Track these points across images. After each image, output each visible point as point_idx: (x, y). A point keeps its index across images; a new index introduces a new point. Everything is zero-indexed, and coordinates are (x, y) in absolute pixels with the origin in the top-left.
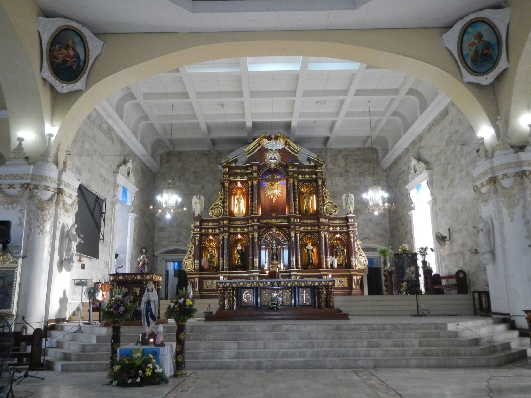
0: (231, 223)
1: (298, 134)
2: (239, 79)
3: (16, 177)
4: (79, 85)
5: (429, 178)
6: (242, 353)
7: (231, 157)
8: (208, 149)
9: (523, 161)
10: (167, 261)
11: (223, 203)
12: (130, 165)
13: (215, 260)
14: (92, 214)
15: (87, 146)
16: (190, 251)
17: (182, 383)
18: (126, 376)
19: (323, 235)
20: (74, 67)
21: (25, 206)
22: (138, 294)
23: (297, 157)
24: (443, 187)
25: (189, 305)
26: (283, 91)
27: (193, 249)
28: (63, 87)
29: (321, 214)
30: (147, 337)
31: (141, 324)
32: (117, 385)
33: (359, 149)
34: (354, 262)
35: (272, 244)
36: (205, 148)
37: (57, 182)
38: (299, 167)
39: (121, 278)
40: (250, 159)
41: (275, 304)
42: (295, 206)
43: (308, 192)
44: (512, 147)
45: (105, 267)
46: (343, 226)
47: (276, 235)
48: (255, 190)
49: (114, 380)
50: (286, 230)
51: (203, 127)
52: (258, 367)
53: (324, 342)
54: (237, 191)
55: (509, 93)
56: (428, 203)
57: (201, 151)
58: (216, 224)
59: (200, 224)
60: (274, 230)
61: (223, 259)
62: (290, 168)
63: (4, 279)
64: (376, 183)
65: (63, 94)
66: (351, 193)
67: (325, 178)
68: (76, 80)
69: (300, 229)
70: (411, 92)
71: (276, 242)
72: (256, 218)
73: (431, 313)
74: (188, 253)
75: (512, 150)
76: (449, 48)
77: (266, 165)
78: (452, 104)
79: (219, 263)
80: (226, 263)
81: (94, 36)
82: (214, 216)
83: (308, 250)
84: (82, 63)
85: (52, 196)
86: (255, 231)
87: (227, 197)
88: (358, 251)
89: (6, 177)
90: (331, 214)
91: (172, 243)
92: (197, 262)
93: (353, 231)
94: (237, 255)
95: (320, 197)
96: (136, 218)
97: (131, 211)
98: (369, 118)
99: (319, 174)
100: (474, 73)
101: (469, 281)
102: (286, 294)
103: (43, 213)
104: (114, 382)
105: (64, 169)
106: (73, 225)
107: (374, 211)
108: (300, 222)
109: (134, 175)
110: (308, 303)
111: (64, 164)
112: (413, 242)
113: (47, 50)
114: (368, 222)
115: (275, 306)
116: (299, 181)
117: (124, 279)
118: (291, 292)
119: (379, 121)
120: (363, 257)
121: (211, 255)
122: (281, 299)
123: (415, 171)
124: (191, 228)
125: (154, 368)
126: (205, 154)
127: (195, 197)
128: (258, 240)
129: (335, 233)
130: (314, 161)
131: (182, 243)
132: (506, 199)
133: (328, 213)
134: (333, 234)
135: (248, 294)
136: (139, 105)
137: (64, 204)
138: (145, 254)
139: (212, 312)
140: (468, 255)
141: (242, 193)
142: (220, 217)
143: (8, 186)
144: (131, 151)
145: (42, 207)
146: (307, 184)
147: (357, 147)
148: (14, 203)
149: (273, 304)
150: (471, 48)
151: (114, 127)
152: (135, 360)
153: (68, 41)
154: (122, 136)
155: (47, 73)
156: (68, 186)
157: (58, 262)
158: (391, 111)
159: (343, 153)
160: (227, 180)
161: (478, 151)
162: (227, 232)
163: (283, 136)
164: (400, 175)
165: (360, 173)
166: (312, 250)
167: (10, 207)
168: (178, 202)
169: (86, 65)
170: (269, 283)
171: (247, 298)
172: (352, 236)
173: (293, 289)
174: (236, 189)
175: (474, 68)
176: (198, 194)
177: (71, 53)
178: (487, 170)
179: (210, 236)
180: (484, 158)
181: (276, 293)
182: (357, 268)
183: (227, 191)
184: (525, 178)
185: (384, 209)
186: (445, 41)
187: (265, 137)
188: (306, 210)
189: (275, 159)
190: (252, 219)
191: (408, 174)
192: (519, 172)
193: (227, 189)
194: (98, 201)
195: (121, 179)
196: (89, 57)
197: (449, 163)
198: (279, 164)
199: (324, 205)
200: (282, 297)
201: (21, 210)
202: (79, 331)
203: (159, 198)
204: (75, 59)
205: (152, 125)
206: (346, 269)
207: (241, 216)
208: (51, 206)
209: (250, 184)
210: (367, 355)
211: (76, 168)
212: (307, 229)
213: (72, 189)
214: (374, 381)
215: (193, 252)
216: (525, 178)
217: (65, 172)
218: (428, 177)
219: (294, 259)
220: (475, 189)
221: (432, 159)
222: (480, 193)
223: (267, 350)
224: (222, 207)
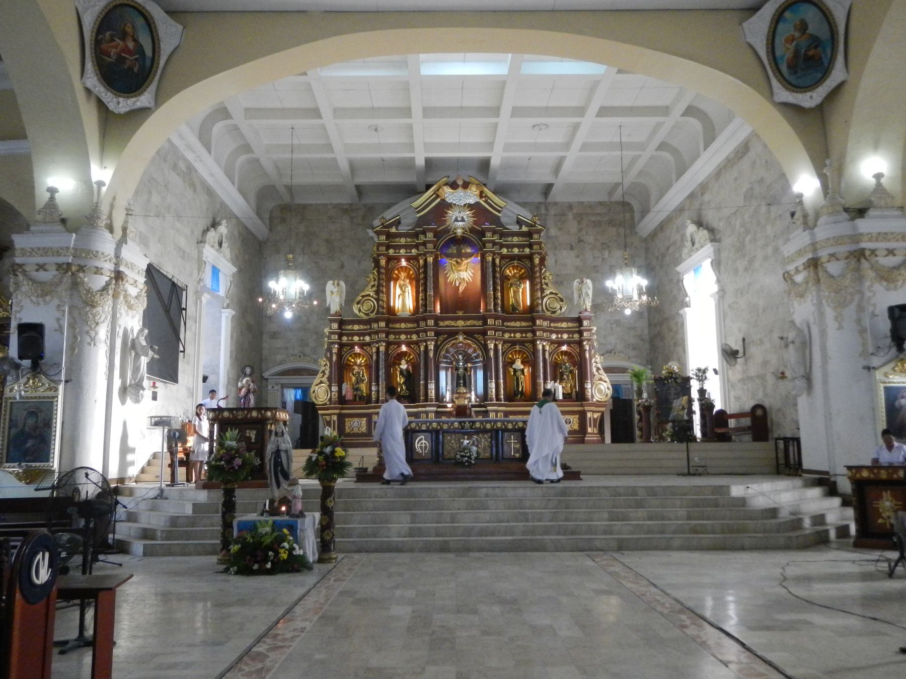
0: (390, 325)
1: (501, 178)
2: (405, 87)
3: (47, 252)
4: (144, 99)
5: (714, 255)
6: (419, 528)
7: (389, 215)
8: (350, 202)
9: (862, 234)
10: (283, 386)
11: (377, 292)
12: (223, 229)
13: (363, 387)
14: (167, 311)
15: (156, 199)
16: (323, 372)
17: (333, 570)
18: (250, 560)
19: (540, 347)
20: (136, 70)
21: (66, 300)
22: (253, 441)
23: (498, 217)
24: (736, 271)
25: (340, 457)
26: (478, 108)
27: (328, 367)
28: (119, 103)
29: (538, 312)
30: (276, 504)
31: (266, 486)
32: (237, 573)
33: (601, 203)
34: (590, 390)
35: (458, 361)
36: (344, 200)
37: (114, 260)
38: (502, 235)
39: (226, 414)
40: (422, 221)
41: (465, 456)
42: (495, 298)
43: (518, 275)
44: (846, 210)
45: (188, 397)
46: (573, 333)
47: (464, 346)
48: (430, 273)
49: (232, 567)
50: (480, 338)
51: (344, 166)
52: (444, 549)
53: (542, 513)
54: (399, 273)
55: (846, 122)
56: (712, 296)
57: (339, 204)
58: (365, 327)
59: (340, 327)
60: (461, 338)
61: (378, 385)
62: (488, 234)
63: (37, 416)
64: (629, 263)
65: (119, 115)
66: (587, 278)
67: (546, 253)
68: (139, 92)
69: (503, 336)
70: (690, 111)
71: (463, 357)
72: (431, 317)
73: (709, 471)
74: (320, 375)
75: (845, 215)
76: (754, 46)
77: (449, 232)
78: (755, 135)
79: (371, 390)
80: (382, 390)
81: (165, 15)
82: (361, 314)
83: (515, 371)
84: (148, 63)
85: (108, 284)
86: (429, 340)
87: (384, 284)
88: (596, 373)
89: (33, 252)
90: (554, 312)
91: (292, 358)
92: (335, 389)
93: (589, 340)
94: (400, 378)
95: (537, 284)
96: (233, 317)
97: (225, 305)
98: (618, 153)
99: (535, 247)
100: (793, 88)
101: (772, 420)
102: (483, 440)
103: (94, 311)
104: (231, 569)
105: (123, 241)
106: (141, 331)
107: (624, 308)
108: (503, 325)
109: (230, 246)
110: (517, 455)
111: (123, 231)
112: (685, 358)
113: (91, 40)
114: (614, 326)
115: (466, 459)
116: (503, 257)
117: (231, 416)
118: (491, 437)
119: (635, 159)
120: (605, 382)
121: (357, 379)
122: (474, 449)
123: (693, 244)
124: (325, 333)
125: (292, 549)
126: (346, 210)
127: (331, 282)
128: (435, 354)
129: (561, 343)
130: (527, 225)
131: (308, 359)
132: (833, 294)
133: (548, 310)
134: (556, 346)
135: (423, 441)
136: (236, 128)
137: (125, 296)
138: (250, 375)
139: (367, 469)
140: (771, 380)
141: (409, 277)
142: (373, 315)
143: (37, 267)
144: (223, 204)
145: (93, 301)
146: (516, 263)
147: (597, 200)
148: (46, 295)
149: (462, 456)
150: (788, 46)
151: (198, 166)
152: (261, 537)
153: (125, 24)
154: (210, 181)
155: (93, 80)
156: (132, 266)
157: (120, 389)
158: (656, 142)
159: (575, 211)
160: (384, 255)
161: (793, 215)
162: (384, 341)
163: (477, 182)
164: (668, 248)
165: (603, 244)
166: (523, 371)
167: (40, 300)
168: (303, 291)
169: (155, 65)
170: (456, 425)
171: (421, 447)
172: (587, 348)
173: (493, 433)
174: (397, 269)
175: (792, 79)
176: (335, 276)
177: (131, 45)
178: (806, 247)
179: (356, 347)
180: (802, 226)
181: (468, 439)
182: (594, 400)
183: (383, 273)
184: (863, 260)
185: (640, 305)
186: (747, 31)
187: (446, 184)
188: (513, 305)
189: (463, 220)
190: (425, 319)
191: (682, 246)
192: (855, 251)
193: (383, 271)
194: (176, 290)
195: (209, 253)
196: (159, 52)
197: (747, 232)
198: (469, 229)
199: (543, 298)
200: (477, 446)
201: (59, 305)
202: (161, 495)
204: (137, 56)
205: (257, 160)
206: (577, 401)
207: (407, 314)
208: (106, 299)
209: (421, 262)
210: (608, 531)
211: (140, 237)
212: (514, 337)
213: (137, 271)
214: (617, 568)
215: (327, 372)
216: (863, 260)
217: (126, 244)
218: (712, 254)
219: (492, 385)
220: (786, 275)
221: (721, 224)
222: (794, 283)
223: (455, 525)
224: (375, 299)
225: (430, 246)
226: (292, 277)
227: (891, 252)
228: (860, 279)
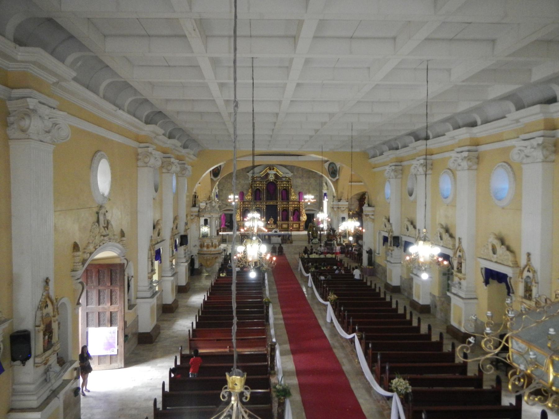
4: (219, 177)
11: (252, 194)
62: (278, 182)
65: (215, 181)
116: (282, 187)
130: (288, 178)
155: (212, 177)
190: (263, 202)
225: (265, 185)
227: (343, 208)
228: (338, 212)
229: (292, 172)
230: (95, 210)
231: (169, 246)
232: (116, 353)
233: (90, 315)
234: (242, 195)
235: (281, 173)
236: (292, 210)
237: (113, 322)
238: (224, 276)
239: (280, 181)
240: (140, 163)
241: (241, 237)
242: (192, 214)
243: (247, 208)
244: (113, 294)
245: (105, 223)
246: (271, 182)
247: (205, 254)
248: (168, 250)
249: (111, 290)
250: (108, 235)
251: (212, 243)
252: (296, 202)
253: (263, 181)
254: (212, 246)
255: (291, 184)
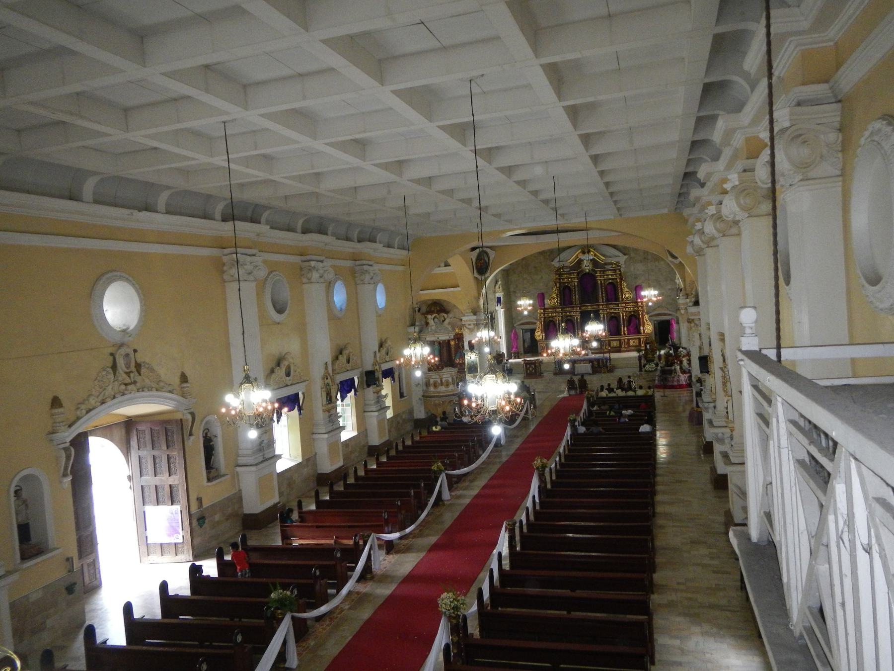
4: (487, 275)
11: (557, 295)
12: (500, 283)
38: (604, 271)
59: (544, 311)
62: (598, 272)
72: (577, 307)
89: (467, 321)
109: (502, 287)
155: (476, 275)
189: (588, 266)
203: (519, 303)
226: (525, 300)
229: (625, 255)
230: (111, 350)
231: (320, 390)
232: (181, 541)
233: (146, 490)
234: (541, 298)
235: (602, 257)
236: (626, 316)
237: (175, 499)
238: (437, 430)
239: (600, 271)
240: (226, 277)
241: (526, 366)
242: (410, 337)
243: (551, 319)
244: (172, 460)
245: (127, 368)
246: (586, 273)
247: (431, 397)
248: (319, 395)
249: (168, 455)
250: (135, 383)
251: (441, 381)
252: (630, 303)
253: (573, 273)
254: (442, 384)
255: (620, 275)
